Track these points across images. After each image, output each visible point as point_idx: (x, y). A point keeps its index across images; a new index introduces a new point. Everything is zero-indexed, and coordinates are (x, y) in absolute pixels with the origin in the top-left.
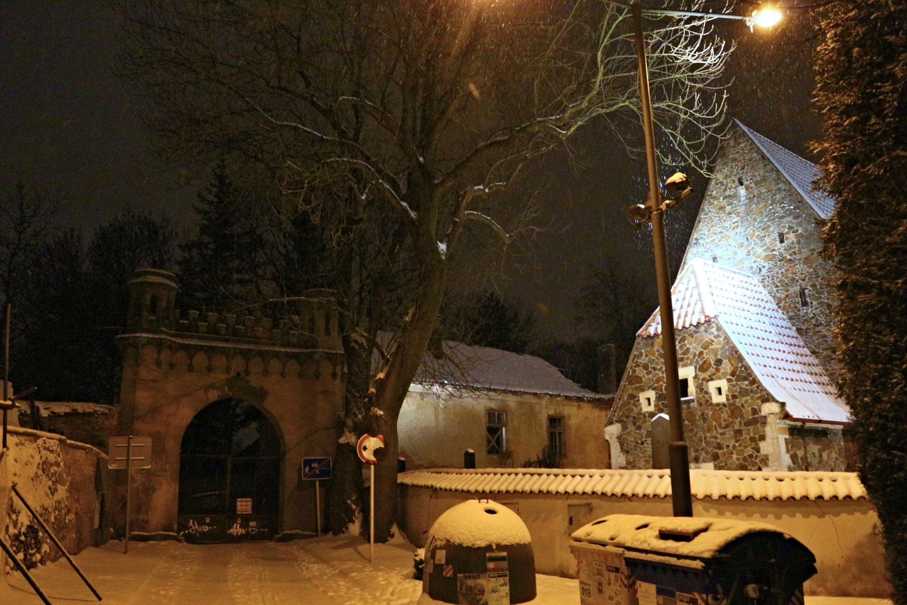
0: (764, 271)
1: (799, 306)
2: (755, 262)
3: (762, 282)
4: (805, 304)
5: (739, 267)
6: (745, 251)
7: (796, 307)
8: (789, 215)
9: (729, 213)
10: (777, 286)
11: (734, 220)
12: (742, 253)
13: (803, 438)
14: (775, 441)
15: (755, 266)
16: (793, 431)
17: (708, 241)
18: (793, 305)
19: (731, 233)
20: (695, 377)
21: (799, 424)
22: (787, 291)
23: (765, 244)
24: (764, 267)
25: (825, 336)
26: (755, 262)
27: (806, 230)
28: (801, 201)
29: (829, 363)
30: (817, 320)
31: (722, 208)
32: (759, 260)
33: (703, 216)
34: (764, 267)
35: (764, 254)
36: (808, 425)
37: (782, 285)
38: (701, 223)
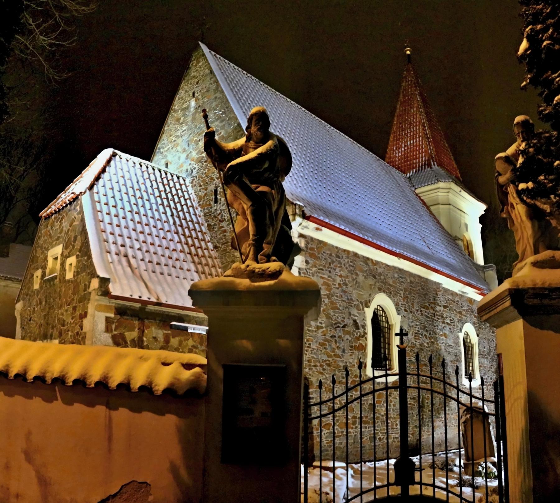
0: (195, 172)
1: (212, 203)
2: (190, 164)
3: (192, 183)
4: (216, 201)
5: (180, 170)
6: (186, 155)
7: (210, 204)
8: (217, 120)
9: (182, 123)
10: (200, 186)
11: (184, 129)
12: (183, 156)
13: (141, 319)
14: (96, 319)
15: (189, 168)
16: (121, 311)
17: (166, 149)
18: (208, 203)
19: (179, 141)
20: (62, 255)
21: (138, 305)
22: (206, 190)
23: (198, 148)
24: (195, 168)
25: (225, 231)
26: (190, 164)
27: (226, 132)
28: (229, 107)
29: (225, 256)
30: (222, 216)
31: (178, 120)
32: (193, 162)
33: (166, 128)
34: (195, 168)
35: (197, 156)
36: (150, 307)
37: (204, 185)
38: (164, 135)
